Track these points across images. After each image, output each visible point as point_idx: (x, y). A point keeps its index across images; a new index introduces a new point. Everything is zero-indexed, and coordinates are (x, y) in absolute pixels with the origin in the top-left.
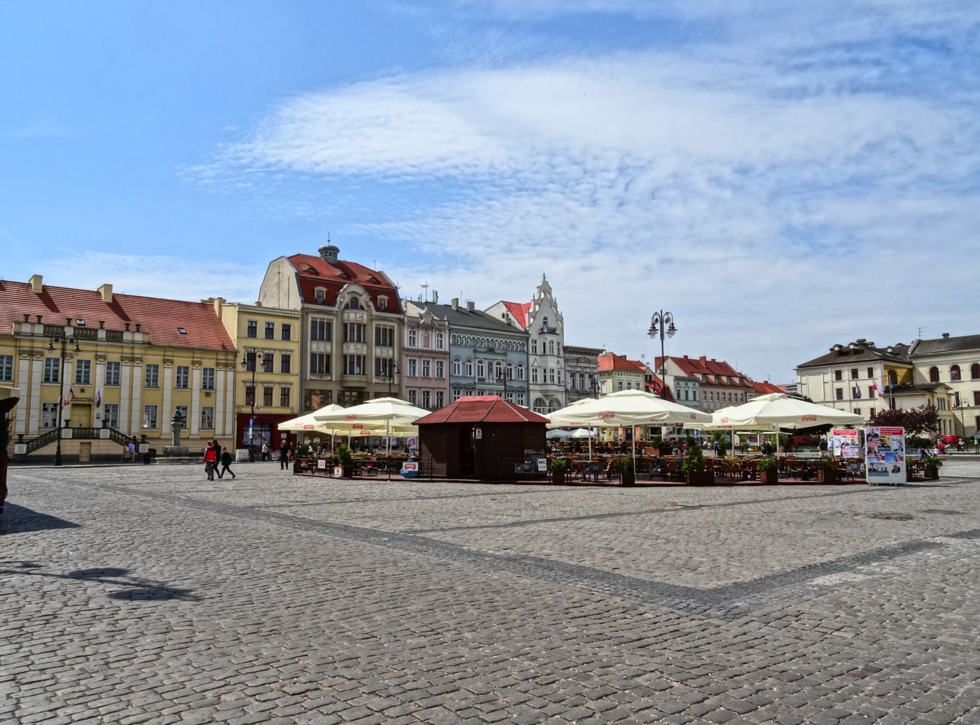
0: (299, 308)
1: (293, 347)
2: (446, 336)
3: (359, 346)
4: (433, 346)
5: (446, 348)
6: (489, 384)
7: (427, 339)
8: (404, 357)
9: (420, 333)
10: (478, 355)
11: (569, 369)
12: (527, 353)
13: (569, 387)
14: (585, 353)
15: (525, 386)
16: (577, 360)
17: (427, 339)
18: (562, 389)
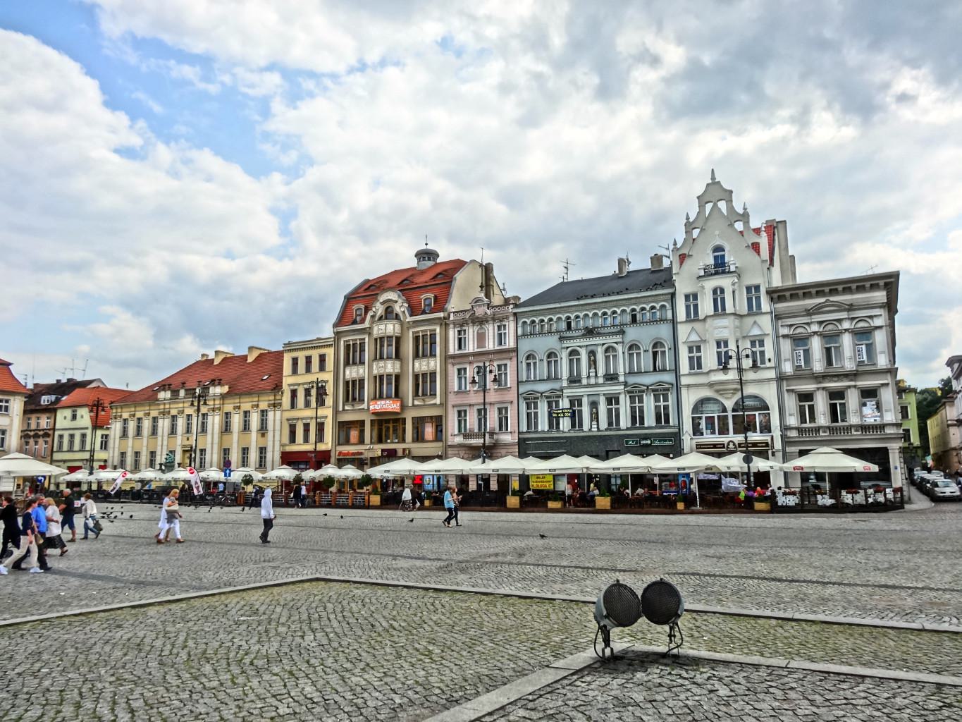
0: (333, 335)
1: (328, 376)
2: (511, 325)
3: (381, 364)
4: (491, 345)
5: (510, 343)
6: (589, 386)
7: (481, 338)
8: (450, 366)
9: (471, 330)
10: (566, 343)
11: (785, 331)
12: (674, 322)
13: (788, 368)
14: (834, 292)
15: (668, 378)
16: (809, 312)
17: (481, 338)
18: (772, 374)
